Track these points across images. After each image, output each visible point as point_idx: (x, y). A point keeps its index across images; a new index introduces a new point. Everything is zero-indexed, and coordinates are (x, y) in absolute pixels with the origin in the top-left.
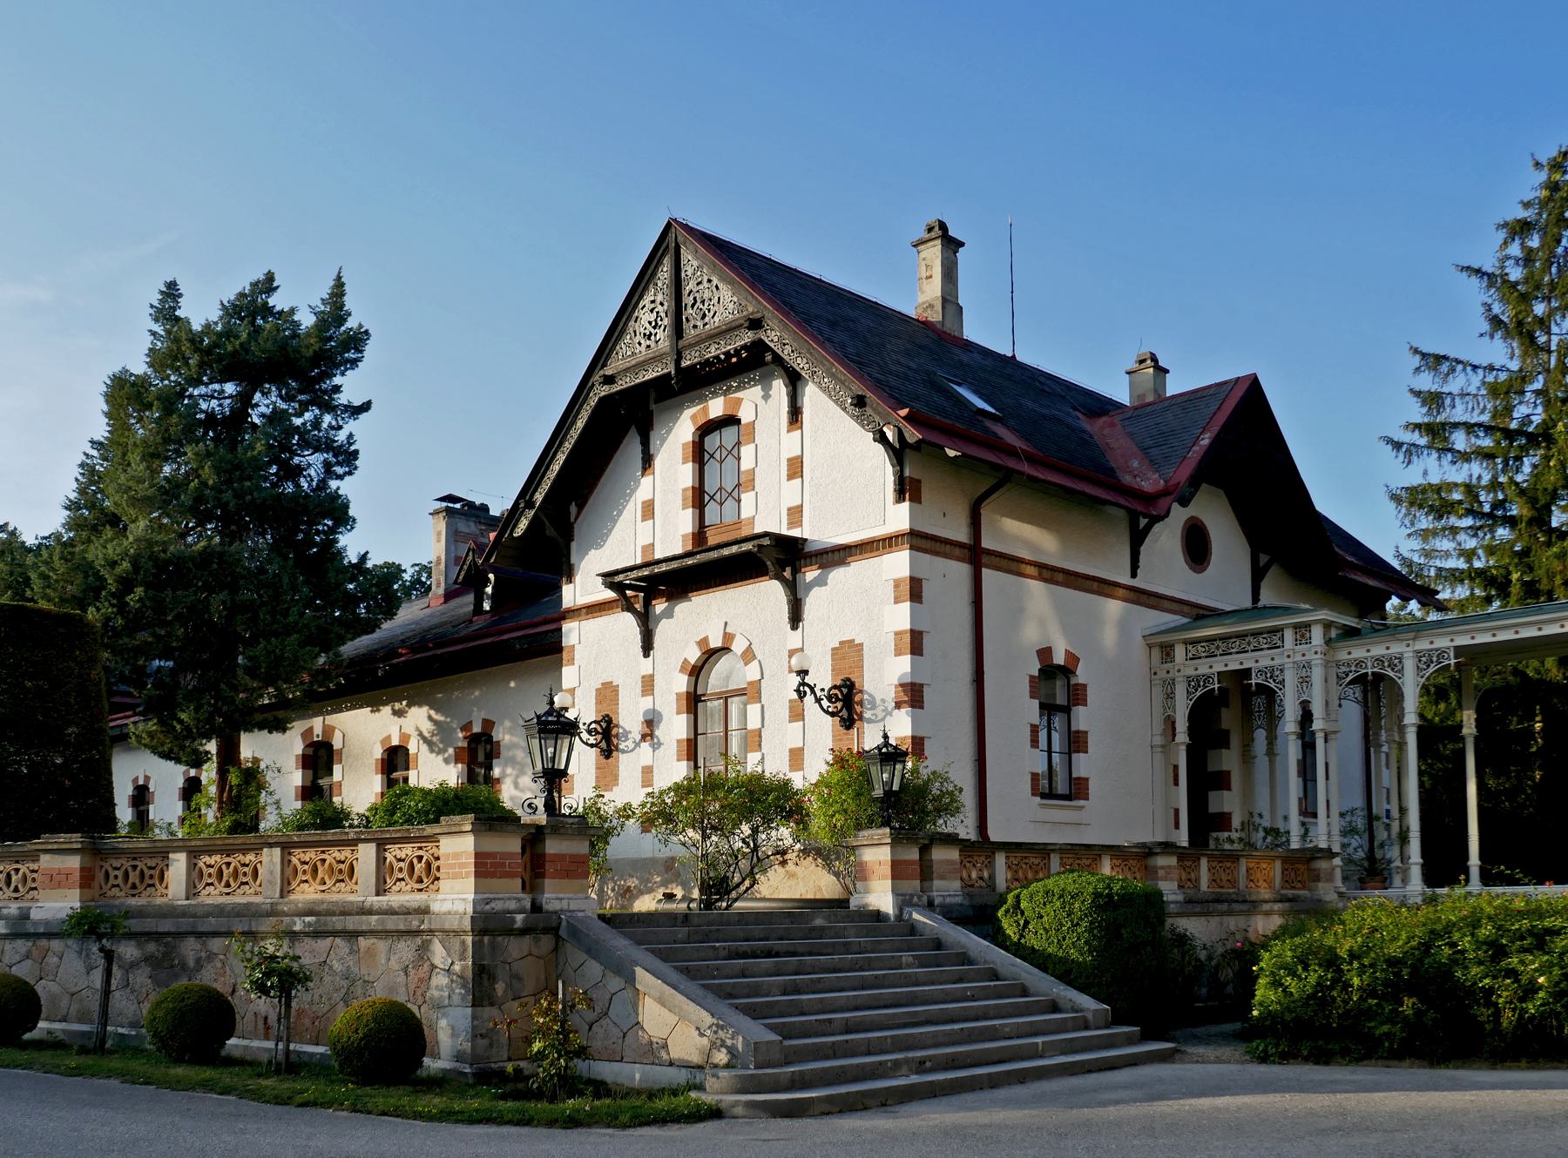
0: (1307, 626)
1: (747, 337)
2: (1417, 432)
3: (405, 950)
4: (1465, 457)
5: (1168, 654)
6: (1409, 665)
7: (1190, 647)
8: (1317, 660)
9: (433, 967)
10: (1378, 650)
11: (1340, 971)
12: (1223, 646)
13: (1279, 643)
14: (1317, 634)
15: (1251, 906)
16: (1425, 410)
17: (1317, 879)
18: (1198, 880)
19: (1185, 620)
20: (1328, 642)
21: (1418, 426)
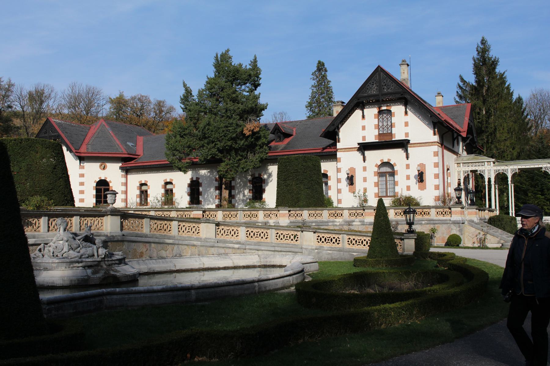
1: (398, 96)
3: (445, 226)
6: (509, 171)
9: (452, 229)
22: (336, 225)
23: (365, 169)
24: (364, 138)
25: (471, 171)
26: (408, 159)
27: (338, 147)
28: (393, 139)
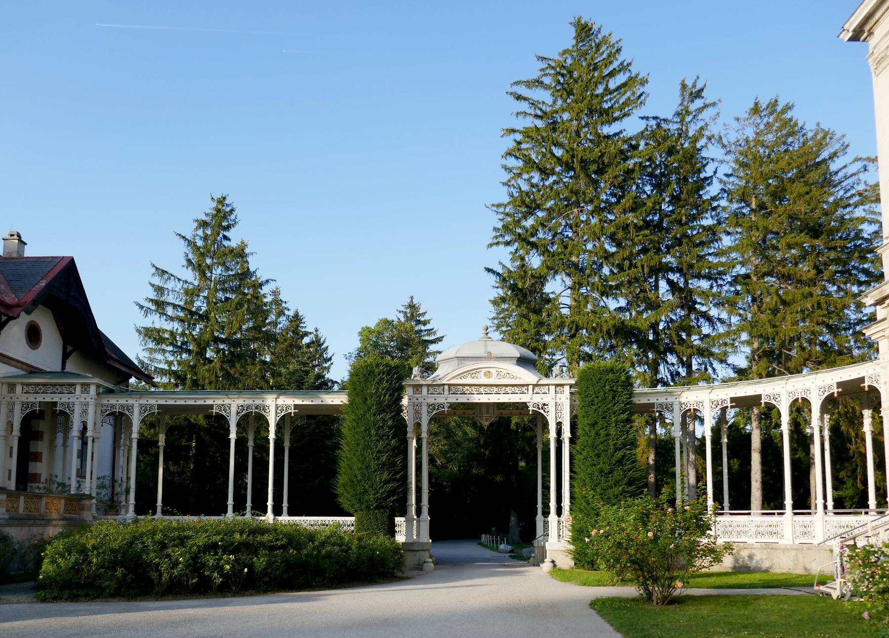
0: (88, 385)
2: (151, 303)
4: (172, 319)
5: (12, 389)
6: (136, 410)
7: (25, 387)
8: (92, 402)
10: (122, 401)
11: (87, 555)
12: (43, 389)
13: (73, 391)
14: (93, 389)
15: (47, 522)
16: (155, 294)
17: (83, 509)
18: (18, 507)
19: (24, 373)
20: (98, 394)
21: (152, 300)
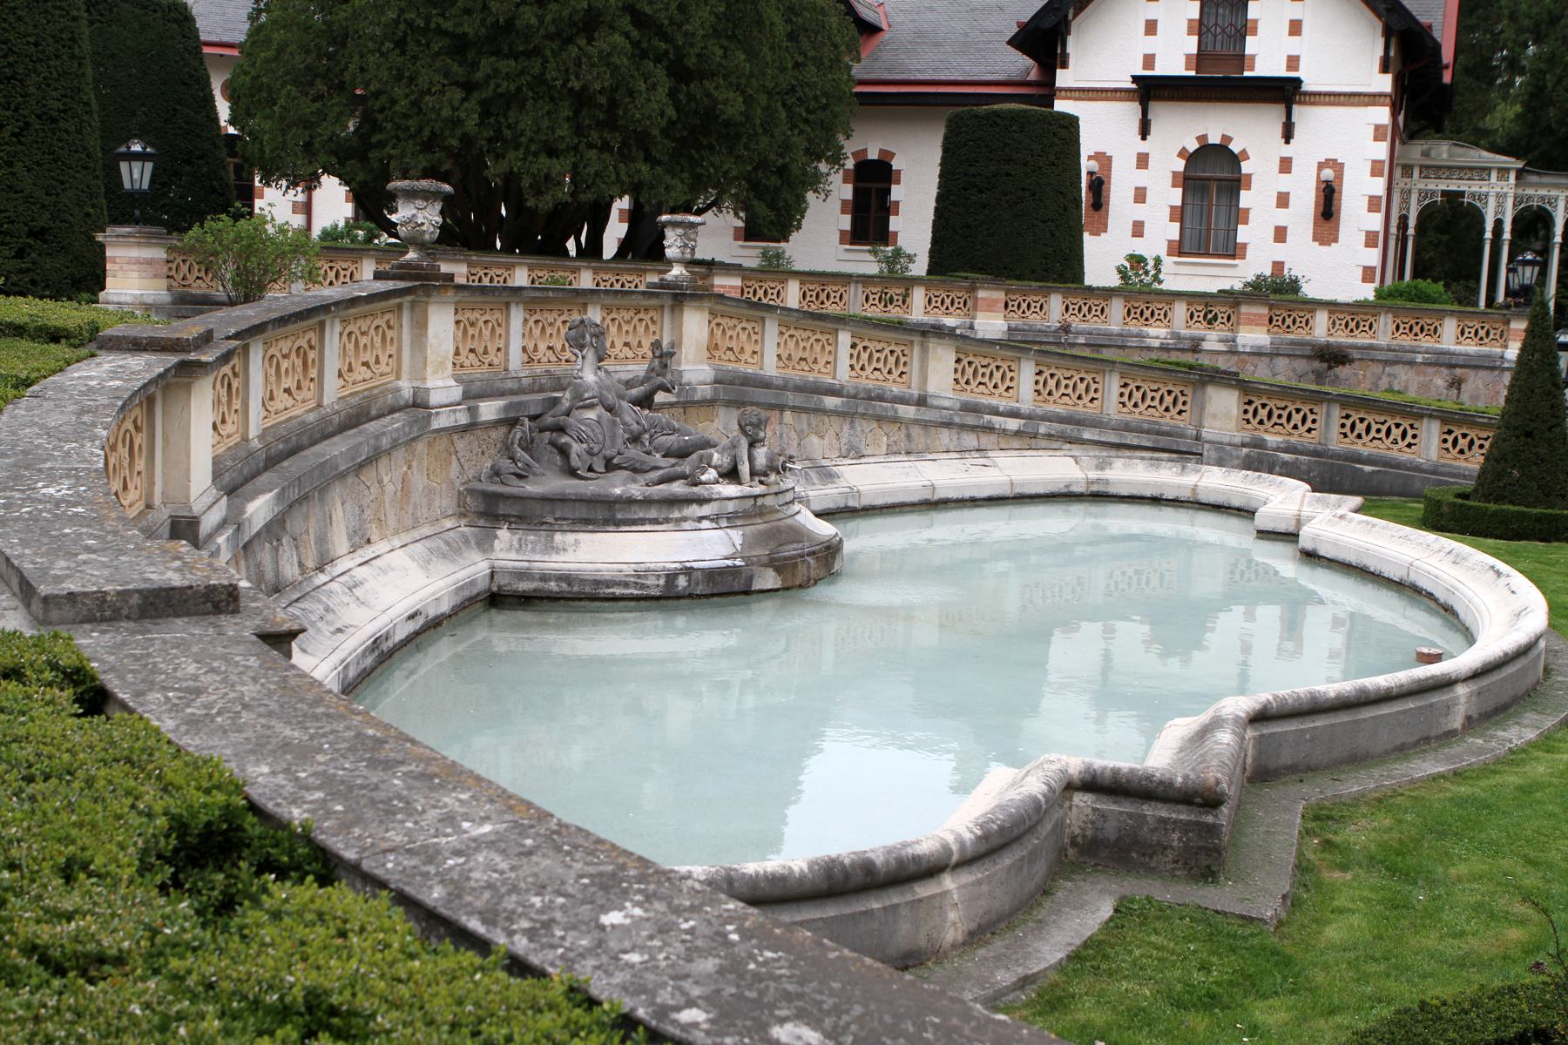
0: (1508, 170)
10: (1542, 192)
14: (1512, 176)
22: (1149, 349)
23: (1143, 161)
24: (1149, 60)
25: (1443, 191)
26: (1287, 142)
27: (1059, 83)
28: (1246, 74)
